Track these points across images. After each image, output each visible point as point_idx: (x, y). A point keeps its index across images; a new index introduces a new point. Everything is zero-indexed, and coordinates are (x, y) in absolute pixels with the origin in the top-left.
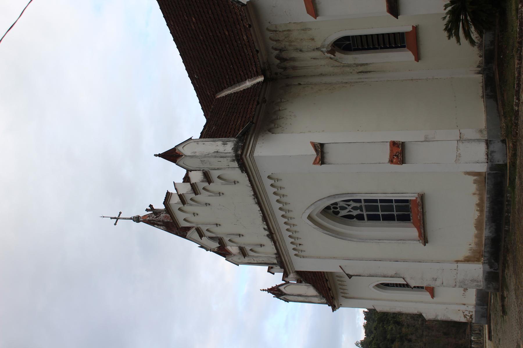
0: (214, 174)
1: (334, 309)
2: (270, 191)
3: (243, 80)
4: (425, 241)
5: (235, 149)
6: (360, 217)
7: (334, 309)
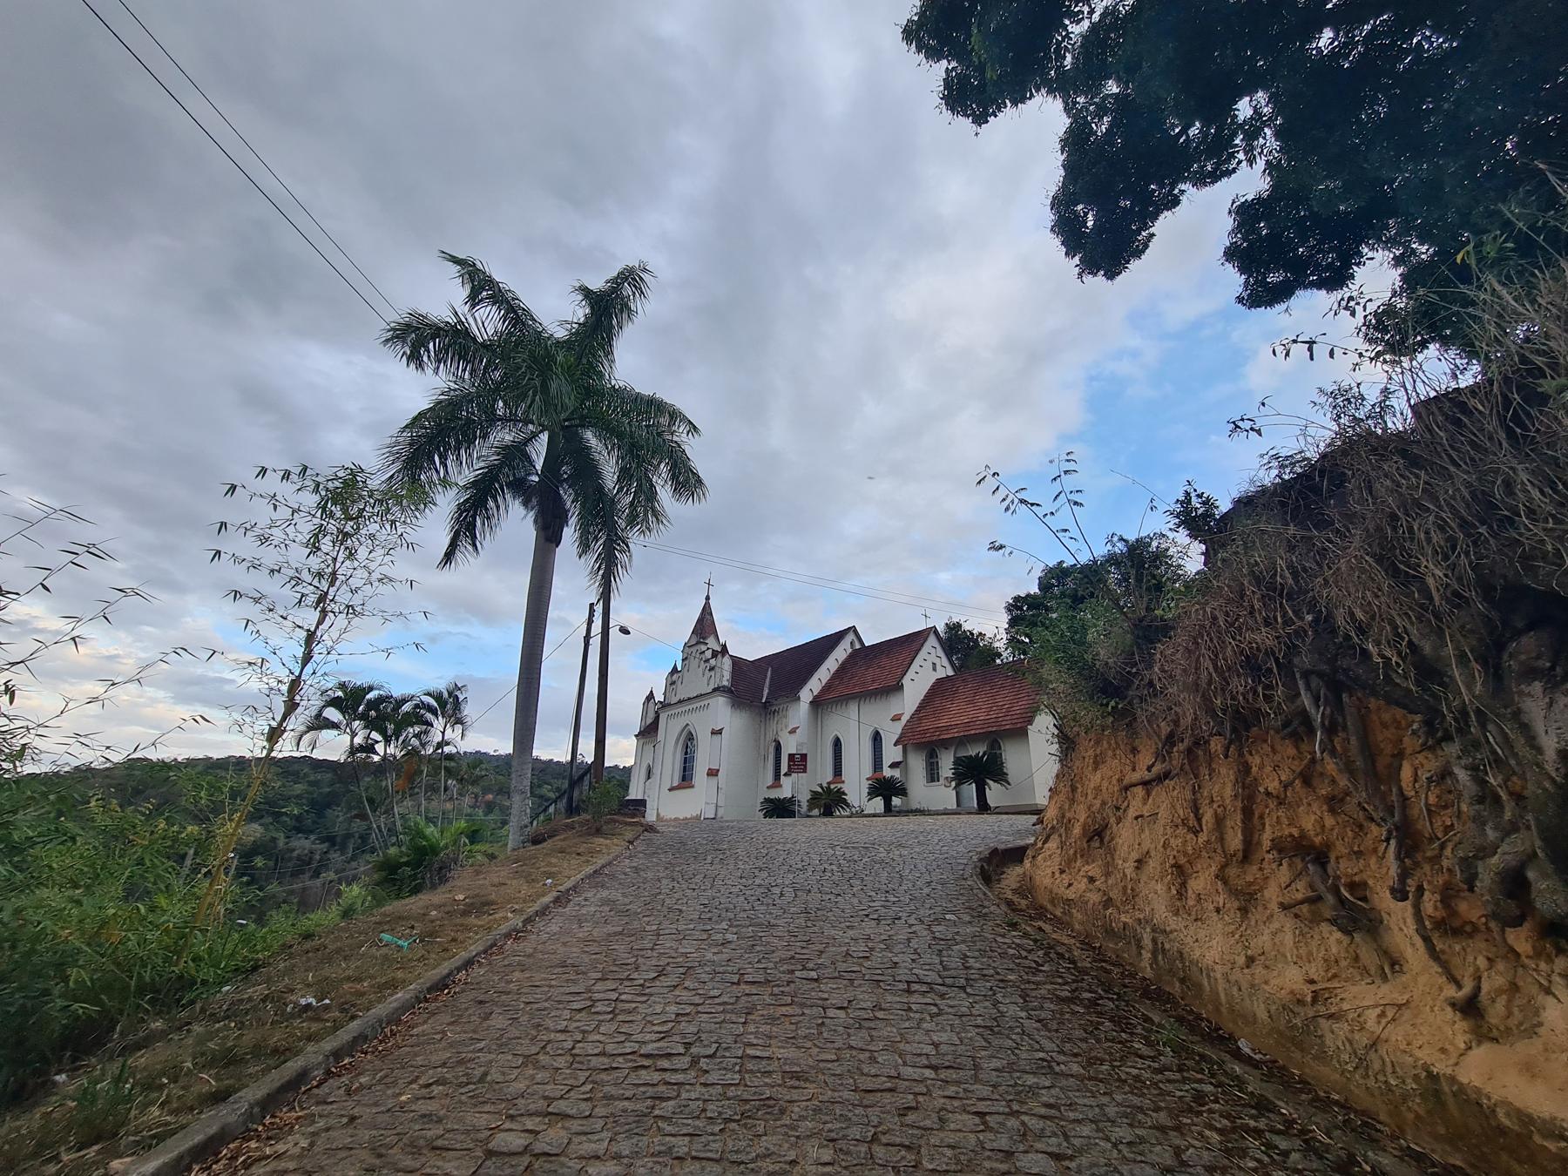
0: (712, 673)
1: (636, 736)
2: (702, 704)
3: (769, 689)
4: (670, 790)
5: (724, 687)
6: (686, 753)
7: (636, 736)
